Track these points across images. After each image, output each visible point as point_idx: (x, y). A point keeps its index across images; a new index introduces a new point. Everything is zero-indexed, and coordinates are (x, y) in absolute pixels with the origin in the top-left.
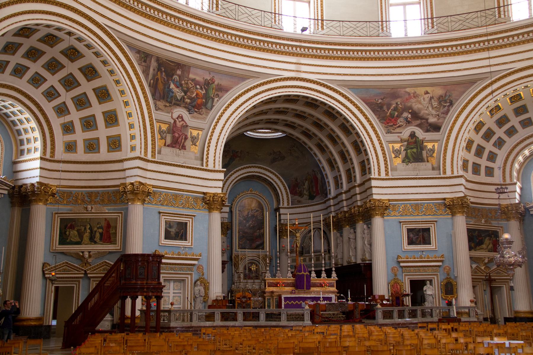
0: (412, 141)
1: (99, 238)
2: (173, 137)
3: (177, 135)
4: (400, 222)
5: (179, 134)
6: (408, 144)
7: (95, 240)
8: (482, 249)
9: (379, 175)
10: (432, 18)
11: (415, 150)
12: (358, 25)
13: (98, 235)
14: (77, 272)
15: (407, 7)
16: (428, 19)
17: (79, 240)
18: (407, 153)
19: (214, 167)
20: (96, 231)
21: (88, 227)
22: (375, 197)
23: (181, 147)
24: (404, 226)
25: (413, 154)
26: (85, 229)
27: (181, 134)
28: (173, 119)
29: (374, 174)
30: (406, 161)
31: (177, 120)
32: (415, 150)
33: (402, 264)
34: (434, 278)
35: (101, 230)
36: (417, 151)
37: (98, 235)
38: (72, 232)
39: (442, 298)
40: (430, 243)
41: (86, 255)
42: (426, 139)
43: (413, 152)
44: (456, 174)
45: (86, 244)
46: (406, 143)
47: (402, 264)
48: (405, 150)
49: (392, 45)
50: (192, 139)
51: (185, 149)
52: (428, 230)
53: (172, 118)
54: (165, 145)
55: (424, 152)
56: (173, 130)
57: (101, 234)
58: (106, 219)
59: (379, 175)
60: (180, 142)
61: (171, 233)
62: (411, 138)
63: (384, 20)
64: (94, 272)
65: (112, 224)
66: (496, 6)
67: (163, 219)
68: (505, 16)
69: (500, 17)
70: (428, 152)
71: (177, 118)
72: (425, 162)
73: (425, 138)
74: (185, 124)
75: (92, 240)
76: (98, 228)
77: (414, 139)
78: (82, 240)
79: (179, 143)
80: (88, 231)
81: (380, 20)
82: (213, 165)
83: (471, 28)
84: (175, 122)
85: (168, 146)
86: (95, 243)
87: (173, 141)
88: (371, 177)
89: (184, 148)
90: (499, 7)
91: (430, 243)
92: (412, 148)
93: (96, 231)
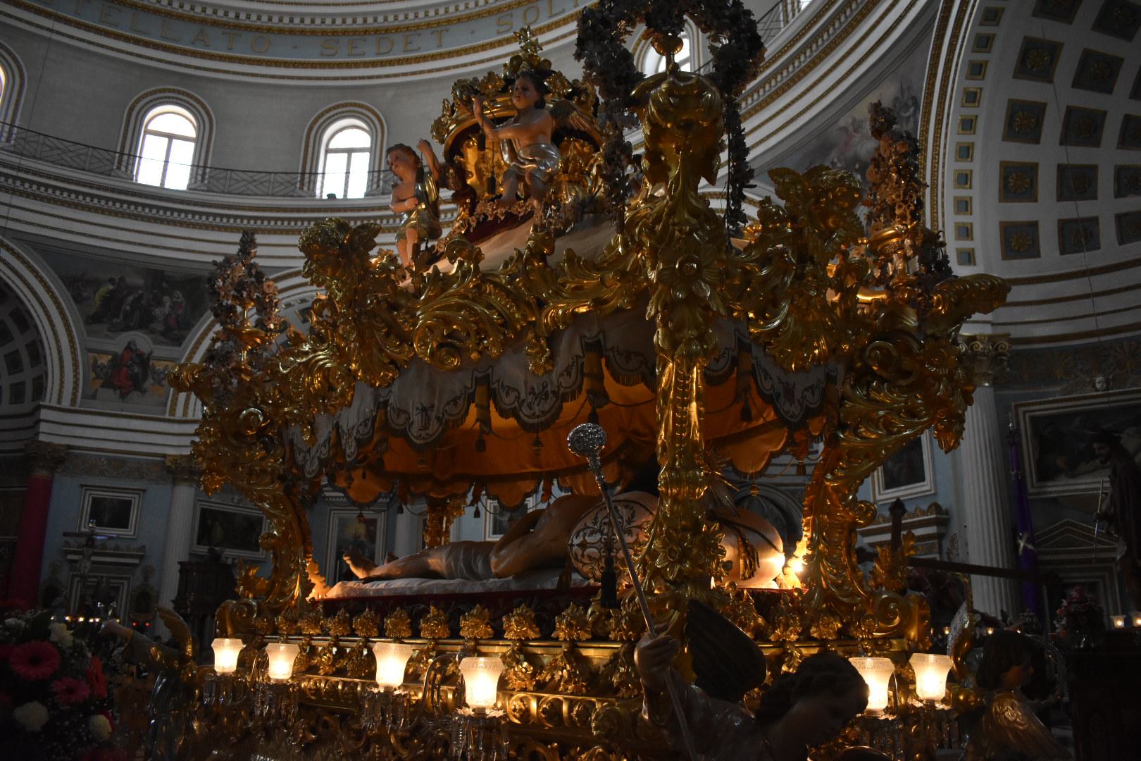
4: (82, 486)
9: (59, 402)
10: (205, 167)
12: (72, 149)
15: (175, 141)
16: (198, 166)
22: (42, 438)
24: (88, 493)
29: (51, 398)
33: (70, 557)
34: (123, 584)
39: (129, 617)
40: (126, 526)
44: (190, 417)
47: (70, 557)
49: (134, 194)
52: (127, 505)
59: (59, 402)
63: (126, 151)
66: (300, 171)
68: (309, 189)
69: (301, 188)
81: (118, 150)
83: (256, 195)
88: (41, 403)
90: (303, 173)
91: (127, 528)
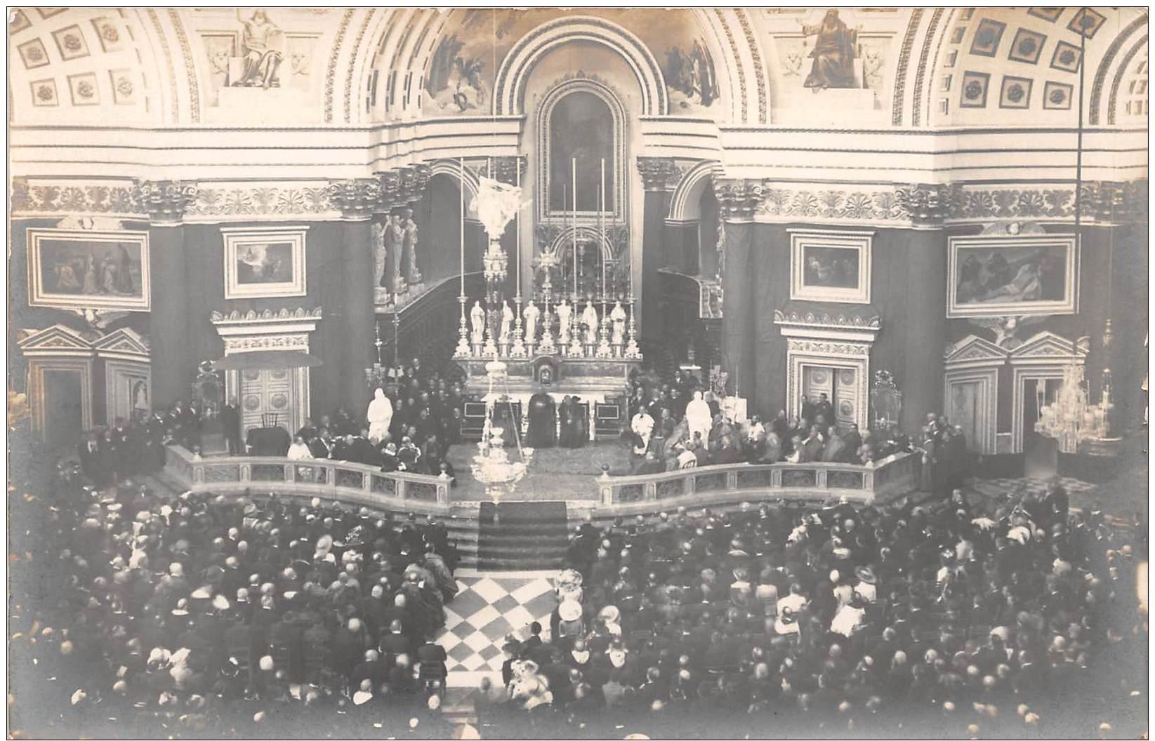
0: (830, 31)
1: (111, 282)
2: (247, 62)
3: (254, 57)
5: (260, 54)
6: (823, 39)
7: (106, 285)
8: (1004, 295)
11: (836, 56)
13: (108, 276)
14: (78, 347)
17: (77, 284)
18: (815, 64)
19: (347, 118)
20: (105, 269)
21: (91, 259)
23: (266, 82)
25: (831, 65)
26: (86, 263)
27: (263, 52)
28: (243, 22)
30: (814, 84)
31: (251, 22)
32: (836, 56)
35: (112, 267)
36: (841, 60)
37: (108, 276)
38: (63, 269)
41: (90, 317)
42: (863, 30)
43: (832, 61)
45: (90, 294)
46: (815, 38)
48: (812, 54)
50: (295, 61)
51: (278, 86)
53: (239, 20)
54: (227, 84)
55: (858, 64)
56: (244, 46)
57: (115, 275)
58: (119, 245)
60: (264, 72)
61: (255, 270)
62: (828, 27)
64: (109, 349)
65: (132, 257)
67: (236, 244)
70: (868, 62)
71: (253, 19)
72: (858, 87)
73: (862, 26)
74: (273, 29)
75: (101, 288)
76: (110, 262)
77: (836, 28)
78: (83, 286)
79: (261, 75)
80: (92, 267)
82: (343, 115)
84: (248, 27)
85: (236, 84)
86: (106, 292)
87: (246, 71)
89: (273, 82)
92: (831, 51)
93: (105, 269)
